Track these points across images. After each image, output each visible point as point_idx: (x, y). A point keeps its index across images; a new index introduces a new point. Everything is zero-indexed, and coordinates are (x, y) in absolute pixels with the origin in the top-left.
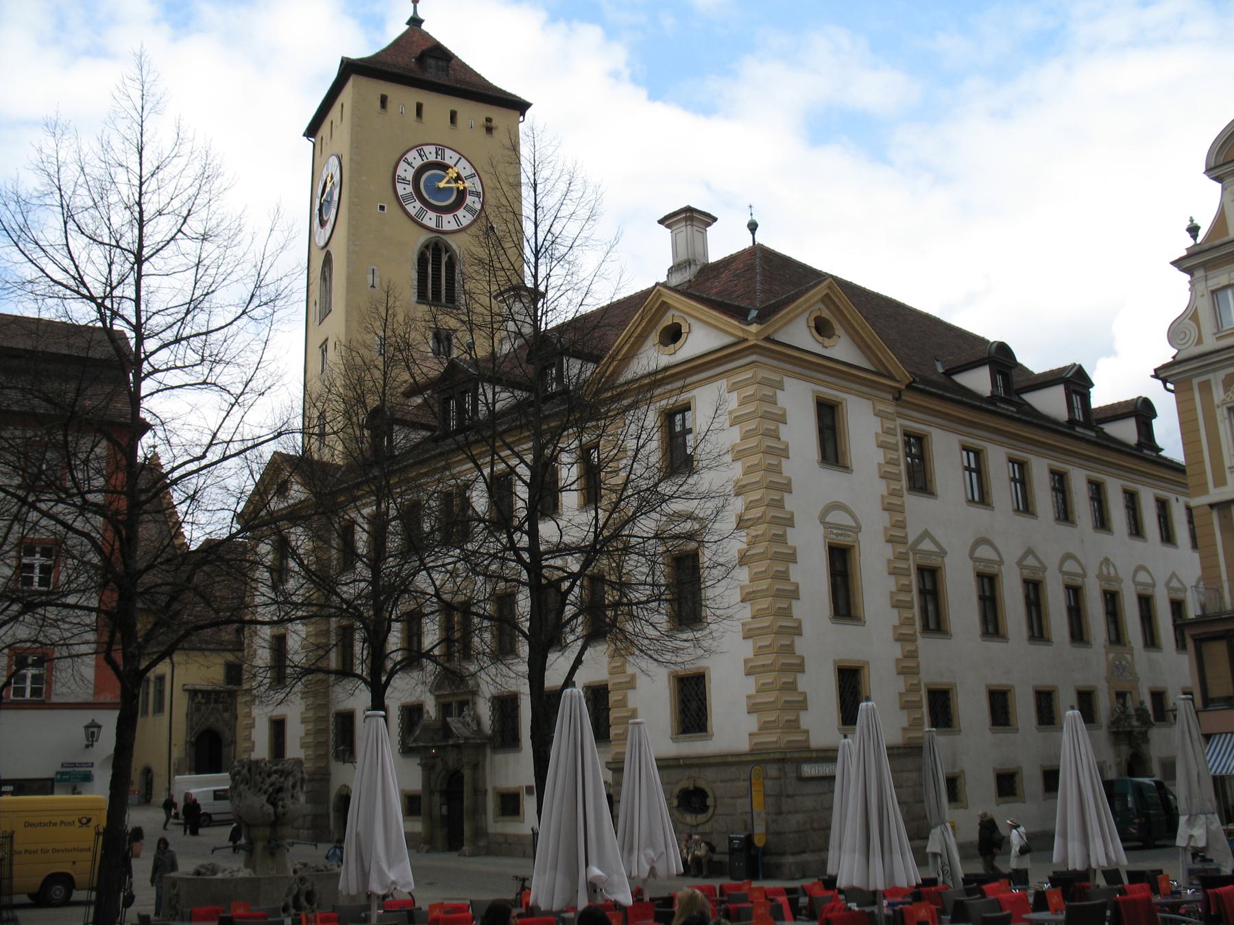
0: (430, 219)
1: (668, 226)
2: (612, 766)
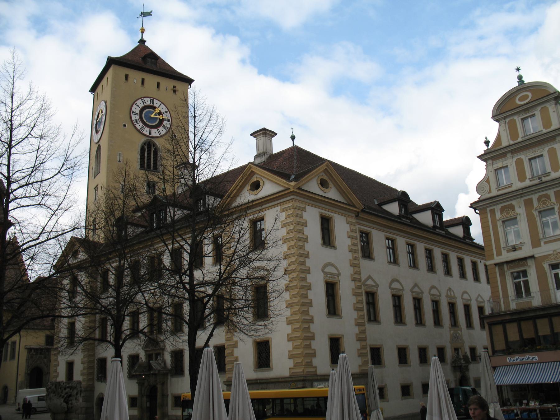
0: (147, 131)
1: (254, 137)
2: (226, 383)
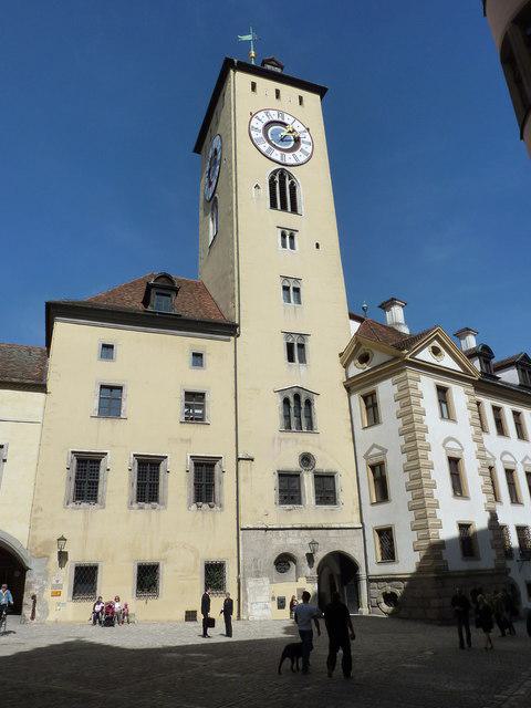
0: (276, 155)
